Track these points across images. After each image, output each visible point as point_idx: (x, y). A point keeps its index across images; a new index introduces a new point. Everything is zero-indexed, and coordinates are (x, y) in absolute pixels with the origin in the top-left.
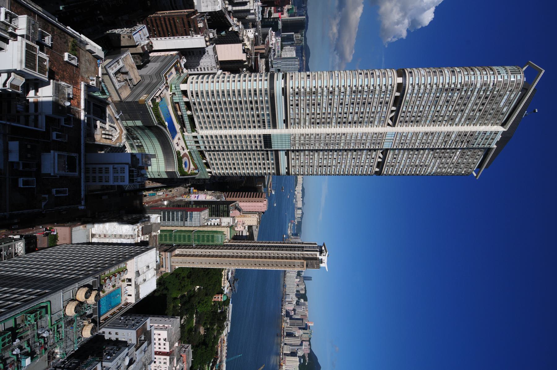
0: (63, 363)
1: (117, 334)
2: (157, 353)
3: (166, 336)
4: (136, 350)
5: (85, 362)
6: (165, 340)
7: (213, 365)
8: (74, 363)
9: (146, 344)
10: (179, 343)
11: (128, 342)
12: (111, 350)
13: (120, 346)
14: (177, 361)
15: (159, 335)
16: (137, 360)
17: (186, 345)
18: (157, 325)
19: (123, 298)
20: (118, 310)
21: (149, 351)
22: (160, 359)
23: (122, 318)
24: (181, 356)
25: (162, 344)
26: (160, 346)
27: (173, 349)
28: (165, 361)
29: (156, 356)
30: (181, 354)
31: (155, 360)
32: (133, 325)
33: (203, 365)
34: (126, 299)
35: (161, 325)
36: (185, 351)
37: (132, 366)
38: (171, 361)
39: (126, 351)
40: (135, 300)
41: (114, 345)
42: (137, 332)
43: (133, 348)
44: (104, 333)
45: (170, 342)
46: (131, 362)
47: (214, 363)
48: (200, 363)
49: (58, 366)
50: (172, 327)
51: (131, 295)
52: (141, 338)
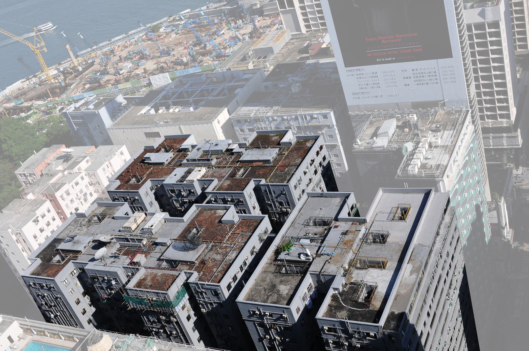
0: (157, 334)
1: (78, 302)
2: (64, 218)
3: (31, 223)
4: (79, 252)
5: (139, 307)
6: (36, 221)
7: (22, 110)
8: (149, 321)
9: (62, 246)
10: (26, 194)
11: (77, 274)
12: (102, 288)
13: (89, 280)
14: (52, 176)
15: (35, 237)
16: (91, 239)
17: (21, 179)
18: (25, 254)
19: (23, 343)
20: (45, 335)
21: (67, 232)
22: (67, 206)
23: (52, 316)
24: (42, 175)
25: (46, 219)
26: (51, 221)
27: (41, 196)
28: (65, 196)
29: (69, 216)
30: (39, 177)
31: (74, 211)
32: (49, 289)
33: (33, 128)
34: (20, 338)
35: (20, 246)
36: (30, 175)
37: (103, 238)
38: (58, 186)
39: (90, 266)
40: (11, 323)
41: (95, 291)
42: (55, 275)
43: (81, 259)
44: (90, 322)
45: (34, 211)
46: (99, 245)
47: (17, 110)
48: (33, 135)
49: (165, 335)
50: (11, 226)
51: (10, 339)
52: (59, 262)
